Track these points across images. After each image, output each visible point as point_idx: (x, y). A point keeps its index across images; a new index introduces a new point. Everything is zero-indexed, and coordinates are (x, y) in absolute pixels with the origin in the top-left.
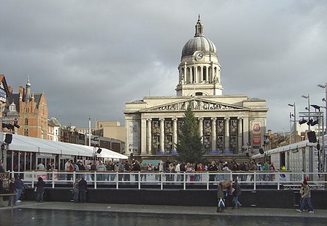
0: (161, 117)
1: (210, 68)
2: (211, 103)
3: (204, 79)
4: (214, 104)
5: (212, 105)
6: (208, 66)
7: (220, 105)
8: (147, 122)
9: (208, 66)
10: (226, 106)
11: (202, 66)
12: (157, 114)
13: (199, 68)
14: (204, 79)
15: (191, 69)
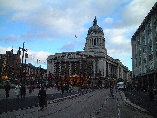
0: (60, 61)
1: (98, 39)
2: (79, 55)
3: (95, 44)
4: (81, 55)
5: (80, 55)
6: (96, 38)
7: (83, 55)
8: (54, 63)
9: (96, 38)
10: (85, 56)
11: (94, 38)
12: (58, 60)
13: (93, 39)
14: (95, 44)
15: (89, 40)
